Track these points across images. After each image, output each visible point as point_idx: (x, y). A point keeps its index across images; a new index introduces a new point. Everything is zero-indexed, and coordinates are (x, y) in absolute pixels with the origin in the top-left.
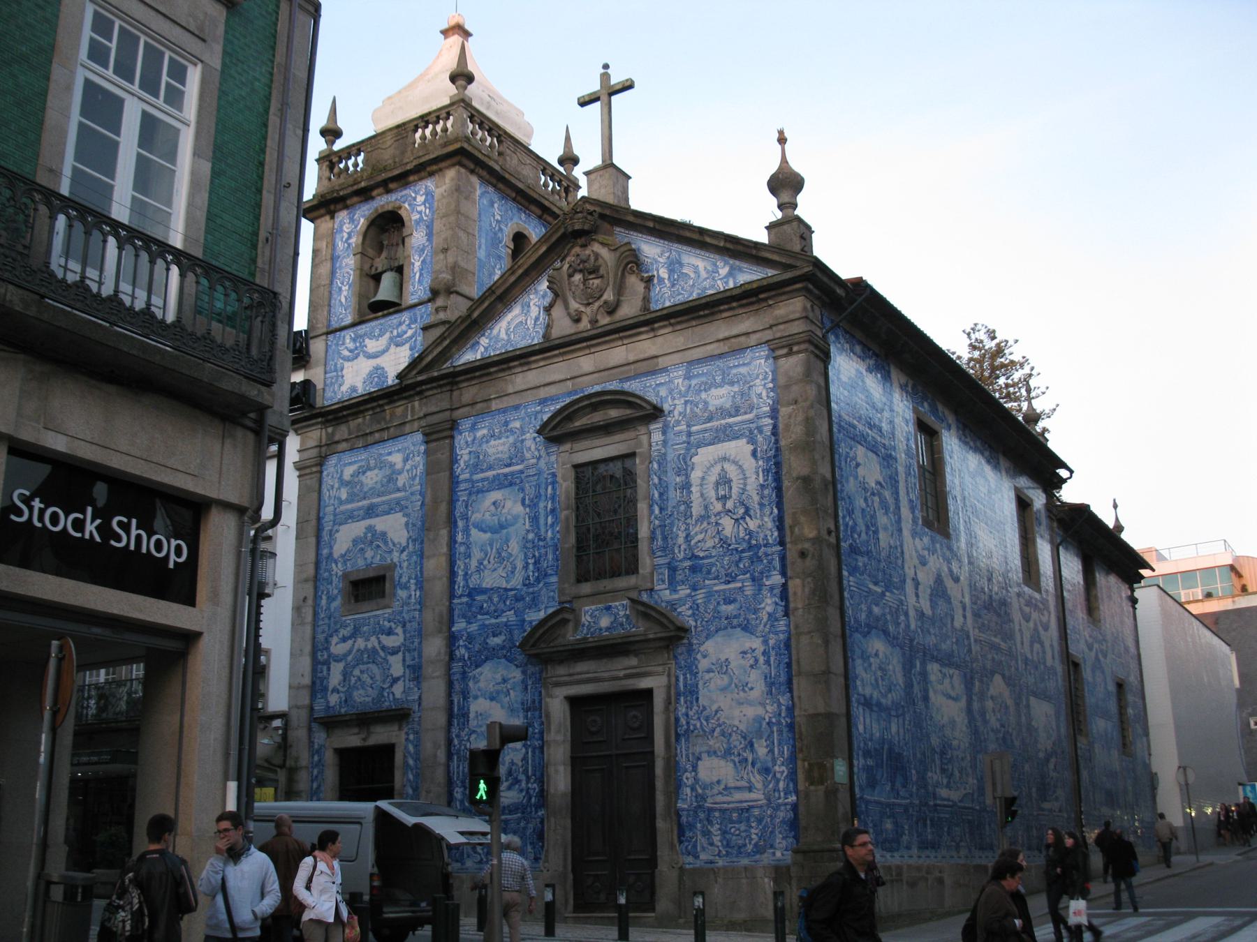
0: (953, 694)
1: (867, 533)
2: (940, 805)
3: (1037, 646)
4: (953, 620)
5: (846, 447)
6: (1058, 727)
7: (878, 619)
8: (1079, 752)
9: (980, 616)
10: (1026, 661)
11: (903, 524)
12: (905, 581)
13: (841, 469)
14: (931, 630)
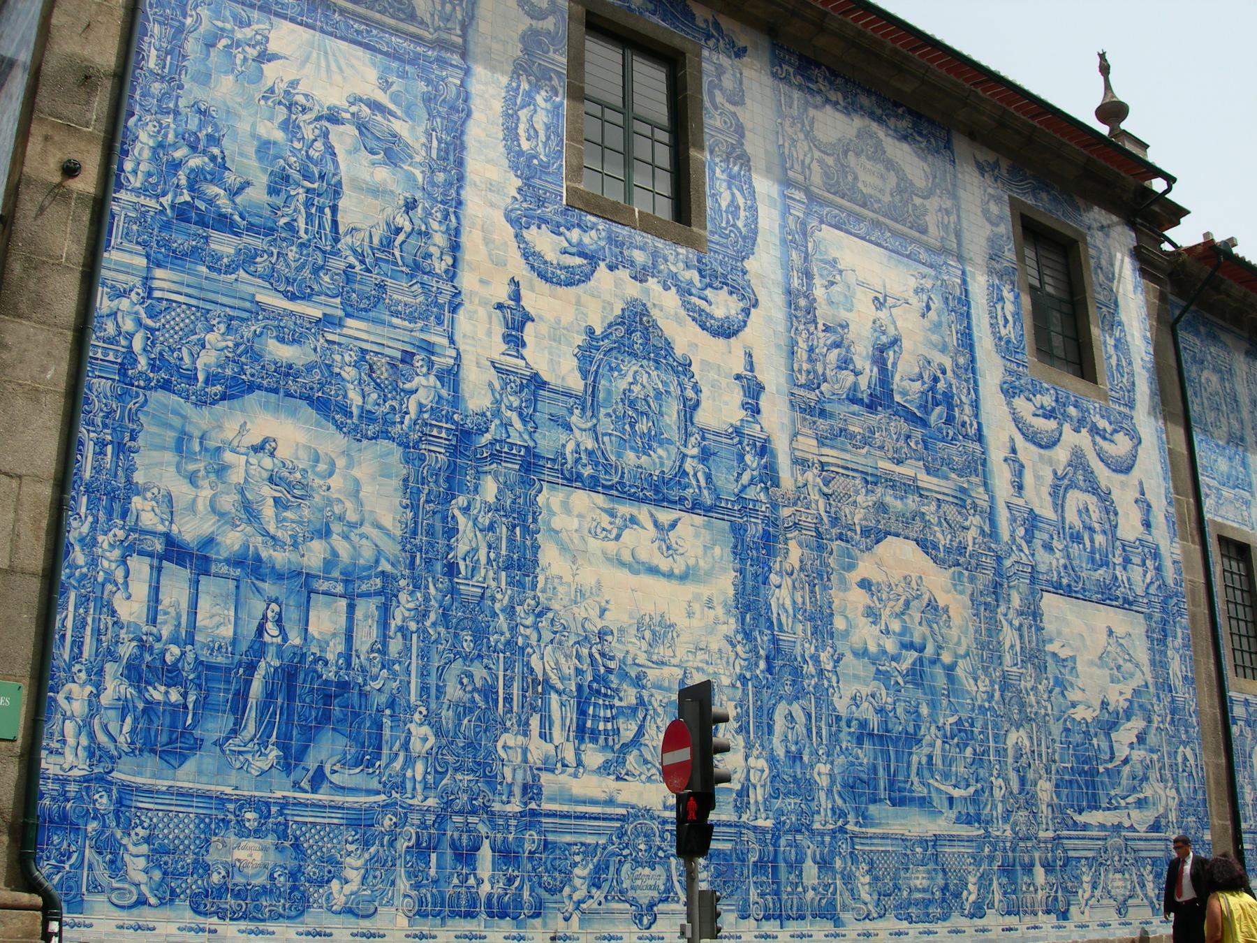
0: (664, 564)
1: (273, 191)
2: (553, 815)
3: (1075, 499)
4: (690, 408)
5: (218, 14)
6: (1159, 664)
7: (288, 371)
8: (1238, 711)
9: (823, 413)
10: (1032, 521)
11: (468, 194)
12: (454, 309)
13: (175, 51)
14: (575, 419)
